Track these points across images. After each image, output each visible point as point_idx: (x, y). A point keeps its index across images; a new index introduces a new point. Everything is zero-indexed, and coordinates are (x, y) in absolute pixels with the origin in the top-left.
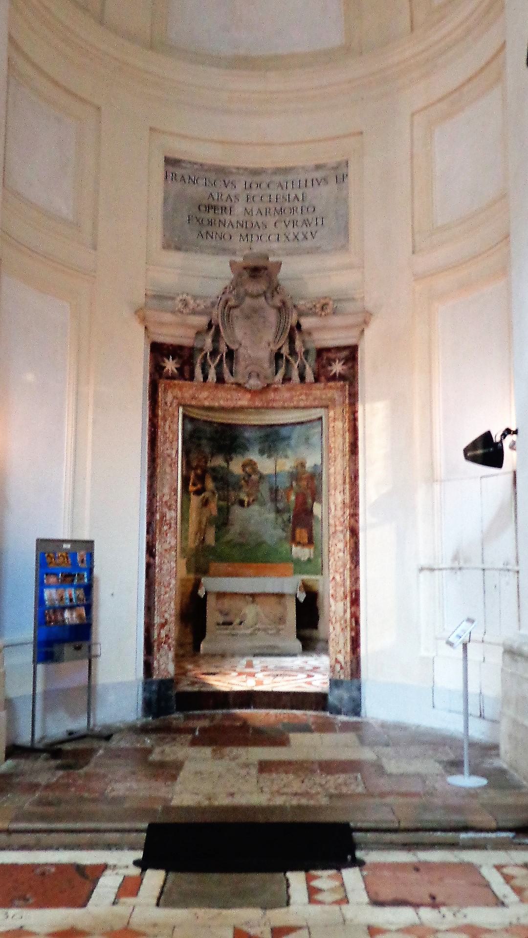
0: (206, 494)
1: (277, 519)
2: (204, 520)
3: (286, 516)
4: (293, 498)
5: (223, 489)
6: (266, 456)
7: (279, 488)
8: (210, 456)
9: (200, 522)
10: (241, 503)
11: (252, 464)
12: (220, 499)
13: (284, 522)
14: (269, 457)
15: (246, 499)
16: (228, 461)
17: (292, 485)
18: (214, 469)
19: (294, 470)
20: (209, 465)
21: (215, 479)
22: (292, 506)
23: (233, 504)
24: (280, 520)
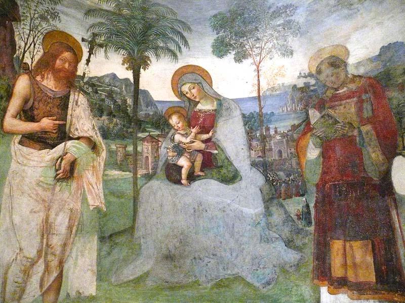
0: (74, 148)
1: (268, 213)
2: (61, 222)
3: (295, 206)
4: (313, 153)
5: (121, 136)
6: (231, 56)
7: (272, 132)
8: (85, 50)
9: (47, 229)
10: (172, 174)
11: (201, 76)
12: (111, 163)
13: (288, 218)
14: (239, 58)
15: (184, 162)
16: (137, 64)
17: (307, 120)
18: (94, 85)
19: (313, 82)
20: (81, 69)
21: (98, 110)
22: (313, 176)
23: (149, 177)
24: (277, 217)
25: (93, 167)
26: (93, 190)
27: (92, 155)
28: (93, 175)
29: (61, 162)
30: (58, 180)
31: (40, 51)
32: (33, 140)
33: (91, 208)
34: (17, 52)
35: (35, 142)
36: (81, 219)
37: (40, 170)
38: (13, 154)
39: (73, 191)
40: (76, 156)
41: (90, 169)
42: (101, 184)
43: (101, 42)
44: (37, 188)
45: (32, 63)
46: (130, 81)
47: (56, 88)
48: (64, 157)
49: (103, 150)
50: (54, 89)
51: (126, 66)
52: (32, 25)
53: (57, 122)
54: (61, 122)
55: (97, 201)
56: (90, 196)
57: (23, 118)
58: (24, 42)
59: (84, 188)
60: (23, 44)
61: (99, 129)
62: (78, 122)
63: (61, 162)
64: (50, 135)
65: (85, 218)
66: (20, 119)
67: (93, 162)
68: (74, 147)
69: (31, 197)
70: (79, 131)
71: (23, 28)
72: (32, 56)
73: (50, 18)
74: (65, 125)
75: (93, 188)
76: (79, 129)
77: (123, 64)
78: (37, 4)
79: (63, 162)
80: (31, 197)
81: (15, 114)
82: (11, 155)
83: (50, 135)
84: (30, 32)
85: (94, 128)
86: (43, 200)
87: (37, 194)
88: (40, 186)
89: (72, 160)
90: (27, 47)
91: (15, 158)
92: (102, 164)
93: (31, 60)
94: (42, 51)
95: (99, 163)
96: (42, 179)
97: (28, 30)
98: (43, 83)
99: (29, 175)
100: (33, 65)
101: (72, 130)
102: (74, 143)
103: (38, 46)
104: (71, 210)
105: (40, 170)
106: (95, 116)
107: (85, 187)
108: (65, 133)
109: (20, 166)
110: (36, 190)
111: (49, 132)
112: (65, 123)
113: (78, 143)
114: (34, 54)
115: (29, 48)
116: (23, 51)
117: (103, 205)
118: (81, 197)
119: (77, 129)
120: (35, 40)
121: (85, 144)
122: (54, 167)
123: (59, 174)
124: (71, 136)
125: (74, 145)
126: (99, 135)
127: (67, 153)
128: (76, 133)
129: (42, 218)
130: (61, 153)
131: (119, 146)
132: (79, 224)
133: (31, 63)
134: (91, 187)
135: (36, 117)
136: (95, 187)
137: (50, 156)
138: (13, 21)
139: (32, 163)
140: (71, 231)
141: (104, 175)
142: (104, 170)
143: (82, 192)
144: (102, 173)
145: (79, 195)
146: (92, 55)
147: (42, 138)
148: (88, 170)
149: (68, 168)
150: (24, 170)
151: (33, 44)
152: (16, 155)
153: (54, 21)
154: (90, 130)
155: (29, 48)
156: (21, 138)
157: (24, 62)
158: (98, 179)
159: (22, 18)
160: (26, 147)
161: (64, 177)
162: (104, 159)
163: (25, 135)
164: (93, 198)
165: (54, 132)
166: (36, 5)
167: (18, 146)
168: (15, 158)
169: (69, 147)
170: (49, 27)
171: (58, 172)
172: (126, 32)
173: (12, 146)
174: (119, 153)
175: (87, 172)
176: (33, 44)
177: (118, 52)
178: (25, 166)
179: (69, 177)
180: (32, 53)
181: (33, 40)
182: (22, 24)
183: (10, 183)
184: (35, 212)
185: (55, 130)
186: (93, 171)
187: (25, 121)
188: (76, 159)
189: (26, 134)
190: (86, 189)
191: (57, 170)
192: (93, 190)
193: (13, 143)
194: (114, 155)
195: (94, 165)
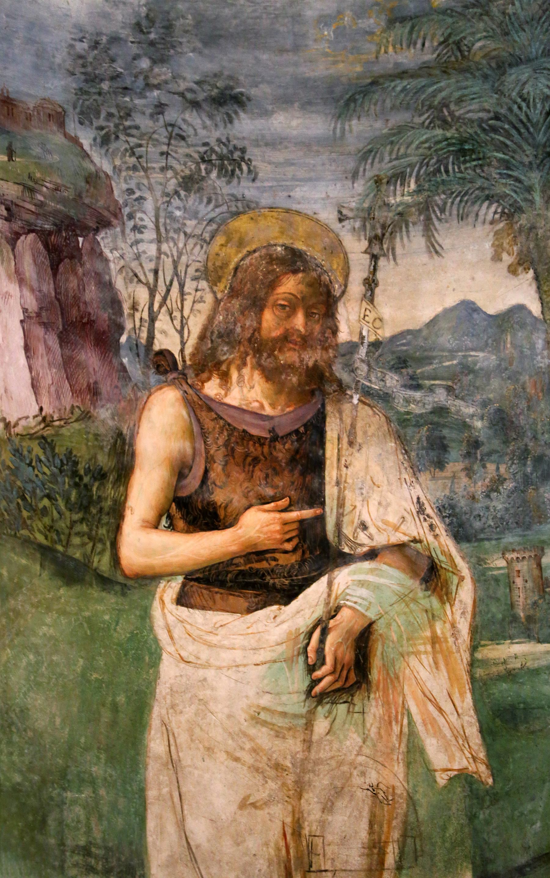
25: (434, 640)
26: (441, 720)
27: (425, 603)
28: (437, 668)
29: (322, 641)
30: (321, 698)
31: (201, 300)
32: (222, 584)
33: (442, 779)
34: (129, 325)
35: (230, 588)
36: (412, 819)
37: (254, 673)
38: (162, 635)
39: (374, 730)
40: (371, 615)
41: (422, 648)
42: (469, 697)
43: (408, 199)
44: (252, 732)
45: (183, 344)
46: (530, 312)
47: (273, 405)
48: (332, 623)
49: (462, 579)
50: (268, 411)
51: (507, 259)
52: (162, 220)
53: (294, 515)
54: (308, 513)
55: (458, 754)
56: (434, 741)
57: (181, 524)
58: (147, 284)
59: (409, 715)
60: (143, 295)
61: (440, 510)
62: (366, 500)
63: (322, 641)
64: (275, 559)
65: (422, 812)
66: (172, 527)
67: (432, 627)
68: (362, 584)
69: (237, 759)
70: (372, 530)
71: (137, 242)
72: (177, 323)
73: (219, 177)
74: (321, 519)
75: (440, 710)
76: (369, 523)
77: (497, 258)
78: (169, 145)
79: (330, 639)
80: (237, 759)
81: (151, 515)
82: (156, 640)
83: (275, 559)
84: (159, 250)
85: (421, 510)
86: (277, 767)
87: (255, 751)
88: (264, 723)
89: (359, 626)
90: (158, 298)
91: (171, 649)
92: (464, 627)
93: (177, 337)
94: (209, 298)
95: (453, 626)
96: (265, 701)
97: (151, 242)
98: (228, 400)
99: (222, 693)
100: (188, 350)
101: (347, 531)
102: (360, 571)
103: (195, 284)
104: (374, 790)
105: (254, 673)
106: (415, 470)
107: (414, 710)
108: (324, 542)
109: (189, 670)
110: (251, 739)
111: (274, 551)
112: (319, 511)
113: (372, 571)
114: (186, 313)
115: (165, 299)
116: (146, 316)
117: (482, 768)
118: (403, 745)
119: (364, 526)
120: (181, 268)
121: (398, 568)
122: (301, 659)
123: (320, 680)
124: (346, 550)
125: (362, 577)
126: (441, 529)
127: (338, 609)
128: (362, 537)
129: (280, 824)
130: (319, 612)
131: (514, 555)
132: (404, 836)
133: (179, 347)
134: (431, 708)
135: (222, 513)
136: (447, 707)
137: (285, 626)
138: (97, 230)
139: (226, 656)
140: (381, 862)
141: (472, 663)
142: (474, 648)
143: (406, 730)
144: (466, 657)
145: (394, 739)
146: (382, 262)
147: (256, 573)
148: (417, 654)
149: (348, 656)
150: (205, 679)
151: (176, 284)
152: (172, 638)
153: (235, 180)
154: (409, 518)
155: (165, 299)
156: (184, 585)
157: (157, 347)
158: (453, 678)
159: (126, 211)
160: (203, 608)
161: (338, 685)
162: (470, 609)
163: (191, 573)
164: (446, 748)
165: (288, 546)
166: (165, 148)
167: (175, 612)
168: (171, 649)
169: (342, 588)
170: (218, 210)
171: (318, 673)
172: (494, 129)
173: (156, 612)
174: (519, 582)
175: (413, 661)
176: (176, 284)
177: (471, 219)
178: (207, 666)
179: (357, 685)
180: (177, 314)
181: (176, 273)
182: (128, 231)
183: (164, 724)
184: (254, 805)
185: (289, 540)
186: (434, 652)
187: (188, 532)
188: (371, 624)
189: (197, 571)
190: (417, 718)
191: (311, 669)
192: (441, 720)
193: (156, 604)
194: (502, 591)
195: (434, 632)
